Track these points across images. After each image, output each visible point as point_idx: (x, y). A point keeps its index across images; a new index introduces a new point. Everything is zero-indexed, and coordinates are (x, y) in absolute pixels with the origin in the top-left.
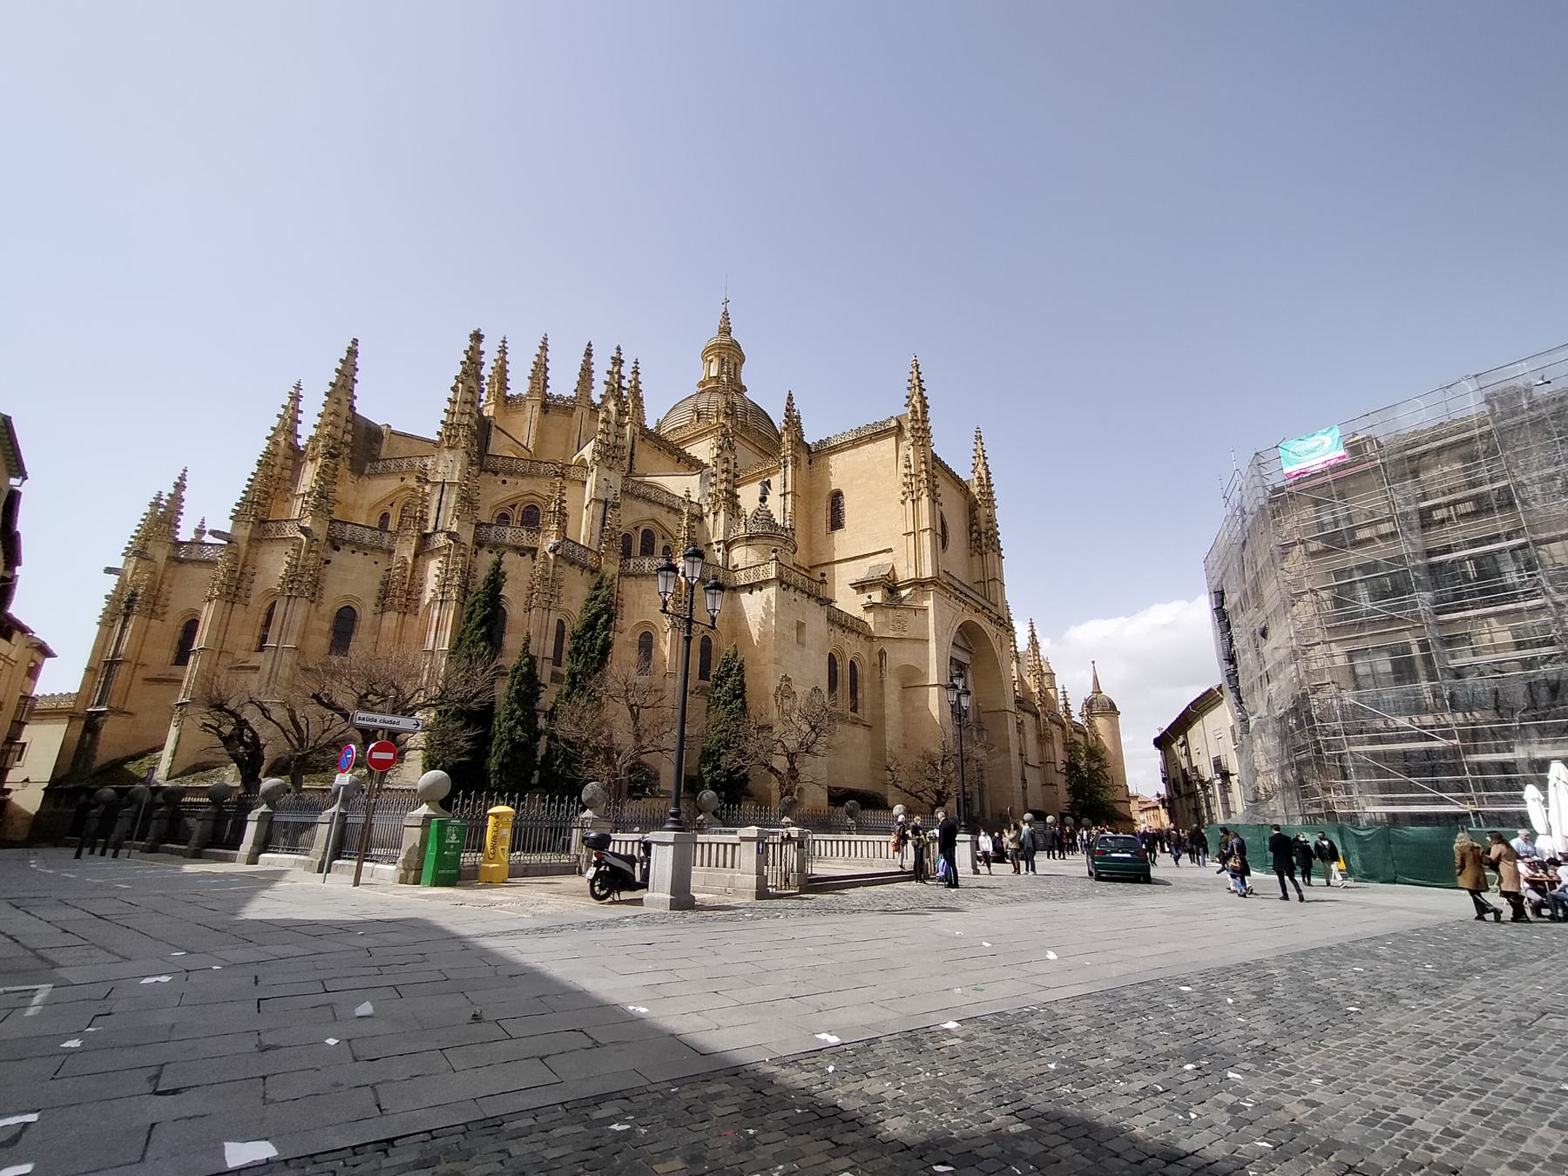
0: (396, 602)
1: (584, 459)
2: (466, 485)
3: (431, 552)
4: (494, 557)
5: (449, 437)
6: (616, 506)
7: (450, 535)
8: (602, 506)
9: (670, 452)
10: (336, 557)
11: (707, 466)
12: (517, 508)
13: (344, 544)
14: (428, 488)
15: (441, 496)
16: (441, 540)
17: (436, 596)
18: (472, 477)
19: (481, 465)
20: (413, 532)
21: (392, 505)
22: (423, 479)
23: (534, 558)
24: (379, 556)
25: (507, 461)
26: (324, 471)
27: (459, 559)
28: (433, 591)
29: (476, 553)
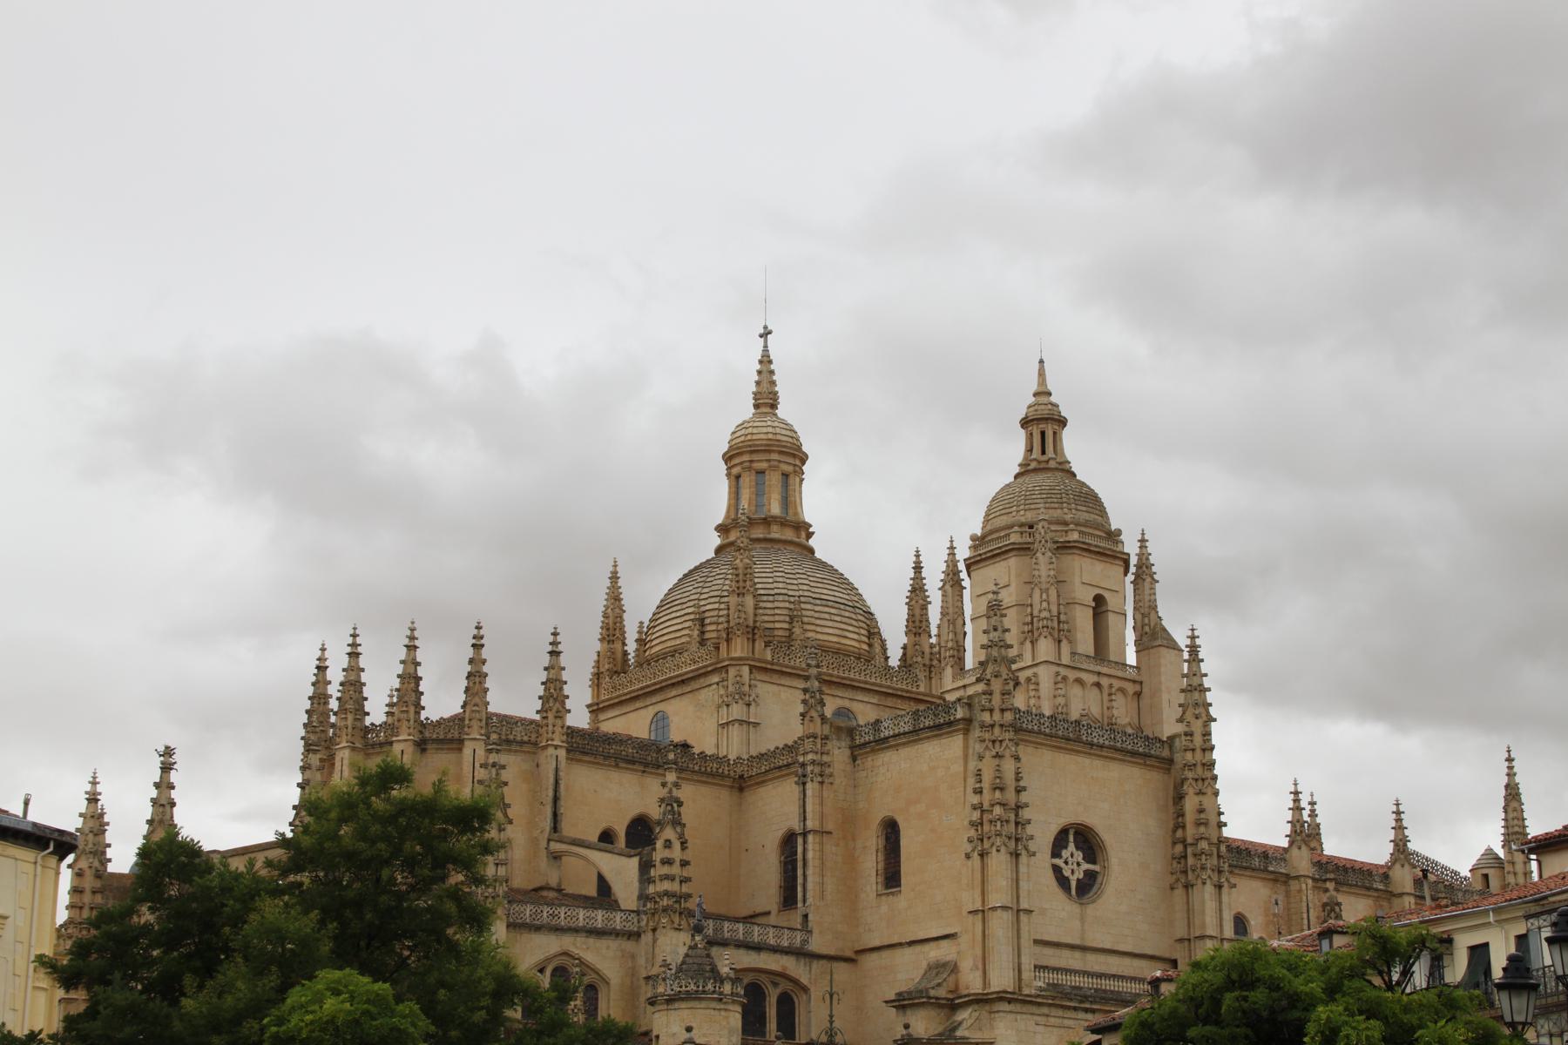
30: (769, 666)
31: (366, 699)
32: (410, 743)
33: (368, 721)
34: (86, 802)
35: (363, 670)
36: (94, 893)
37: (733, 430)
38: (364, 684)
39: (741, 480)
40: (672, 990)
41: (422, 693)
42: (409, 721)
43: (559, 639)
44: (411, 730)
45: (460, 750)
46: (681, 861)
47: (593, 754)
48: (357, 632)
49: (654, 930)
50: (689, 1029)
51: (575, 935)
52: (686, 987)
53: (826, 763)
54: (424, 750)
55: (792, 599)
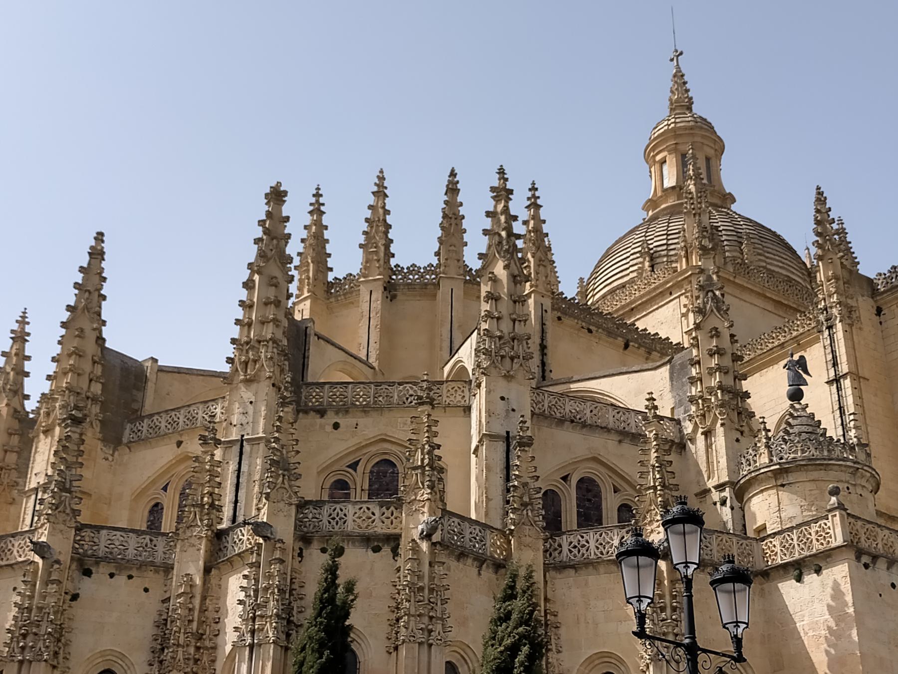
0: (180, 655)
1: (464, 369)
2: (277, 440)
3: (230, 561)
4: (325, 559)
5: (246, 364)
6: (526, 443)
7: (259, 528)
8: (501, 446)
9: (610, 333)
10: (86, 586)
11: (679, 348)
12: (360, 468)
13: (97, 563)
14: (218, 454)
15: (240, 464)
16: (245, 538)
17: (241, 638)
18: (285, 426)
19: (298, 403)
20: (201, 531)
21: (165, 489)
22: (210, 440)
23: (395, 552)
24: (151, 579)
25: (338, 390)
26: (64, 447)
27: (275, 568)
28: (236, 629)
29: (300, 555)
30: (732, 279)
31: (329, 255)
32: (381, 283)
33: (331, 277)
34: (11, 341)
35: (326, 228)
36: (10, 434)
37: (655, 126)
38: (327, 241)
39: (666, 168)
40: (781, 459)
41: (391, 241)
42: (378, 261)
43: (537, 194)
44: (381, 269)
45: (434, 296)
46: (732, 354)
47: (575, 318)
48: (320, 192)
49: (708, 434)
50: (835, 492)
51: (606, 435)
52: (803, 451)
53: (852, 307)
54: (393, 298)
55: (739, 235)
